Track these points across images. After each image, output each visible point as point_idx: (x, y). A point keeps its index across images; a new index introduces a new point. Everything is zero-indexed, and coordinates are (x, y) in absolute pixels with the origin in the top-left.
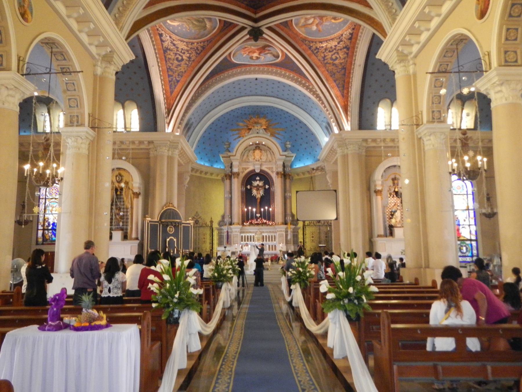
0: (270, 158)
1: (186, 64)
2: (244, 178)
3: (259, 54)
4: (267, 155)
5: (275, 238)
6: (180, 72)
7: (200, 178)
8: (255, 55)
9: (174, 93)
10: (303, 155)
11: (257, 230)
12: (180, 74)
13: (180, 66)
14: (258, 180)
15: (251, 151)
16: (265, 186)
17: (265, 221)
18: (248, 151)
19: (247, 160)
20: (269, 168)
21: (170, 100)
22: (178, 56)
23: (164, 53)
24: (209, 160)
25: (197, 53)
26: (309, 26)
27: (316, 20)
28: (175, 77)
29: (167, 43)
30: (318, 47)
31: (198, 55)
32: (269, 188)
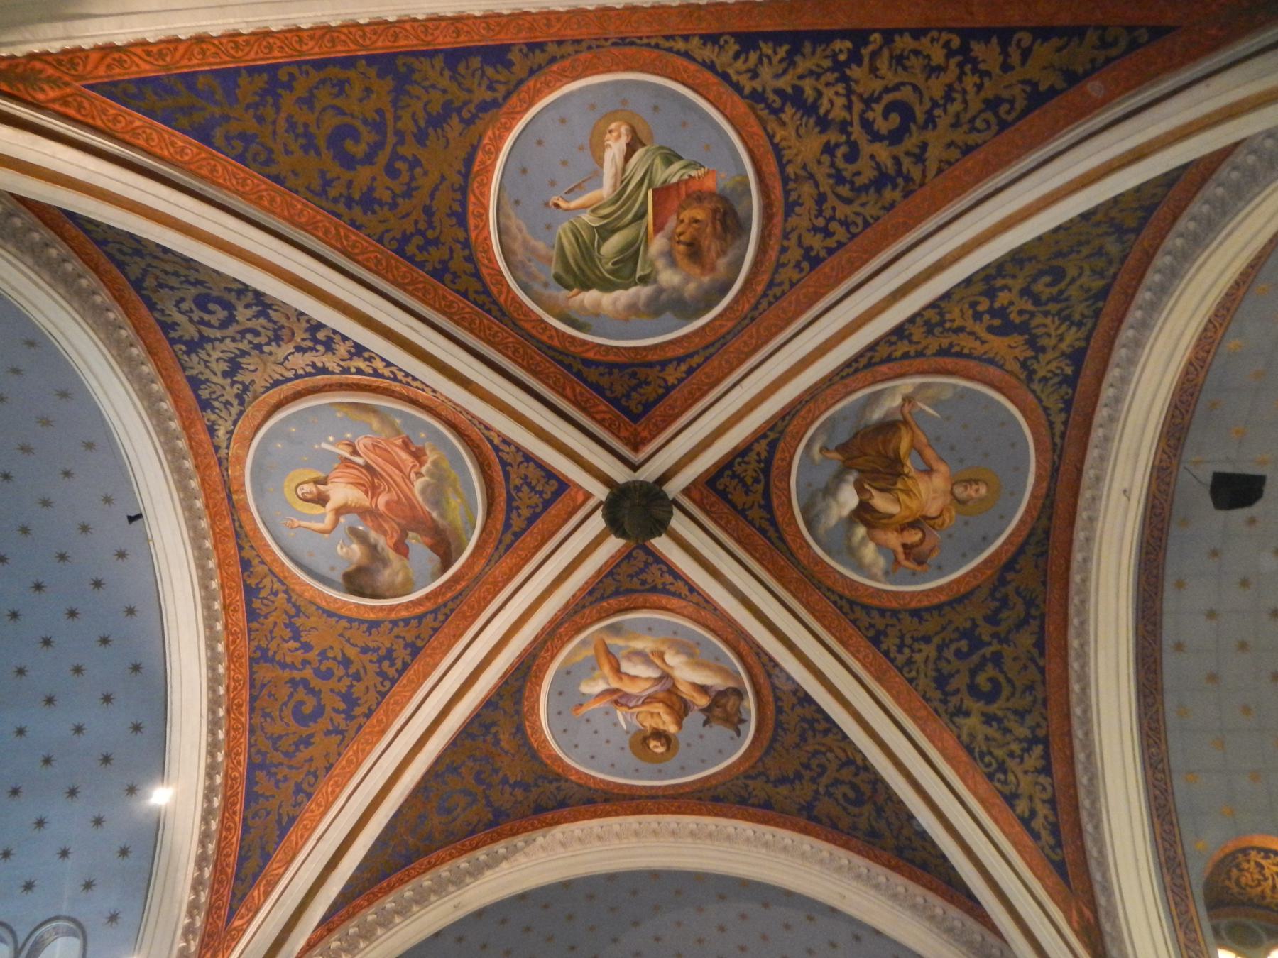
1: (327, 183)
3: (340, 511)
6: (270, 151)
8: (342, 492)
9: (113, 108)
12: (254, 147)
13: (305, 149)
21: (52, 81)
22: (368, 136)
23: (371, 59)
25: (405, 239)
26: (606, 669)
27: (647, 685)
28: (226, 118)
29: (445, 82)
30: (493, 730)
31: (395, 245)
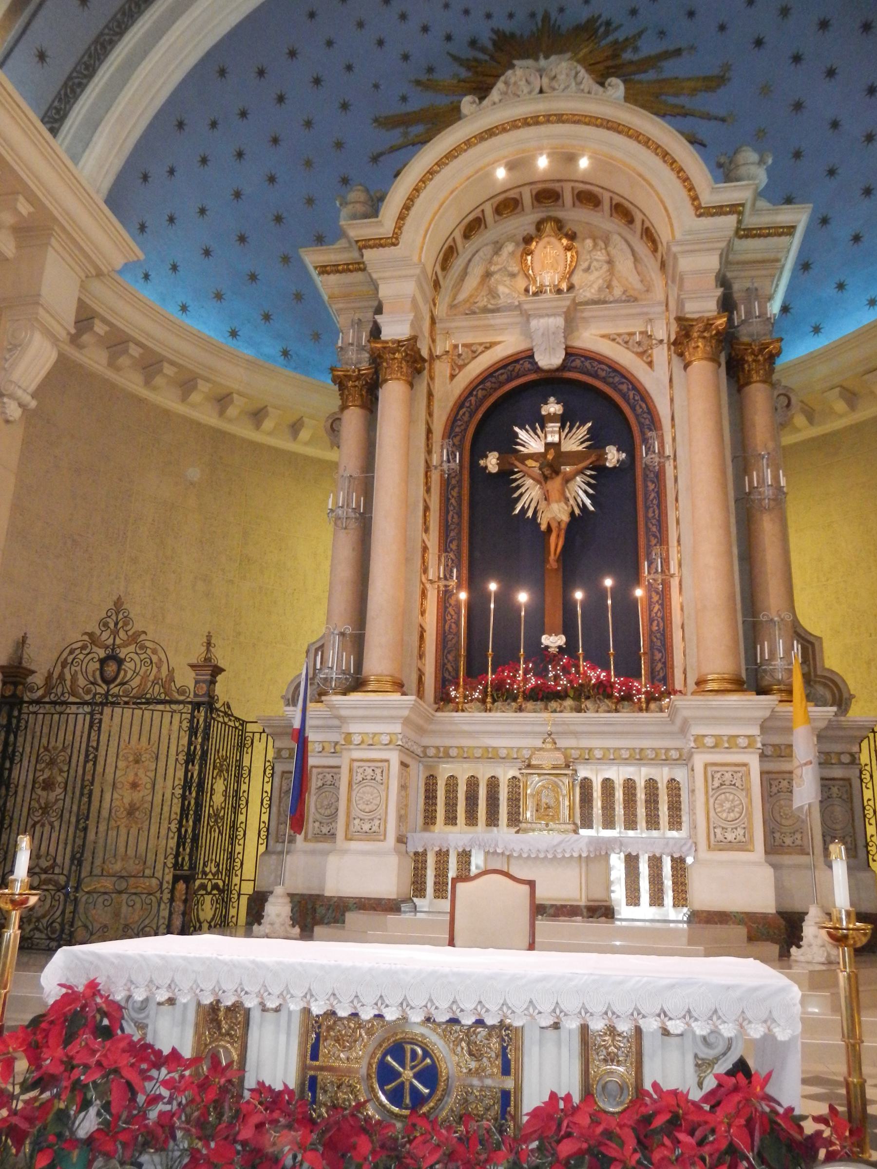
0: (634, 280)
2: (460, 404)
4: (610, 262)
5: (675, 808)
7: (219, 436)
10: (841, 286)
11: (538, 743)
14: (552, 418)
15: (510, 247)
16: (602, 457)
17: (595, 675)
18: (488, 250)
19: (482, 301)
20: (625, 339)
24: (285, 353)
32: (627, 468)
